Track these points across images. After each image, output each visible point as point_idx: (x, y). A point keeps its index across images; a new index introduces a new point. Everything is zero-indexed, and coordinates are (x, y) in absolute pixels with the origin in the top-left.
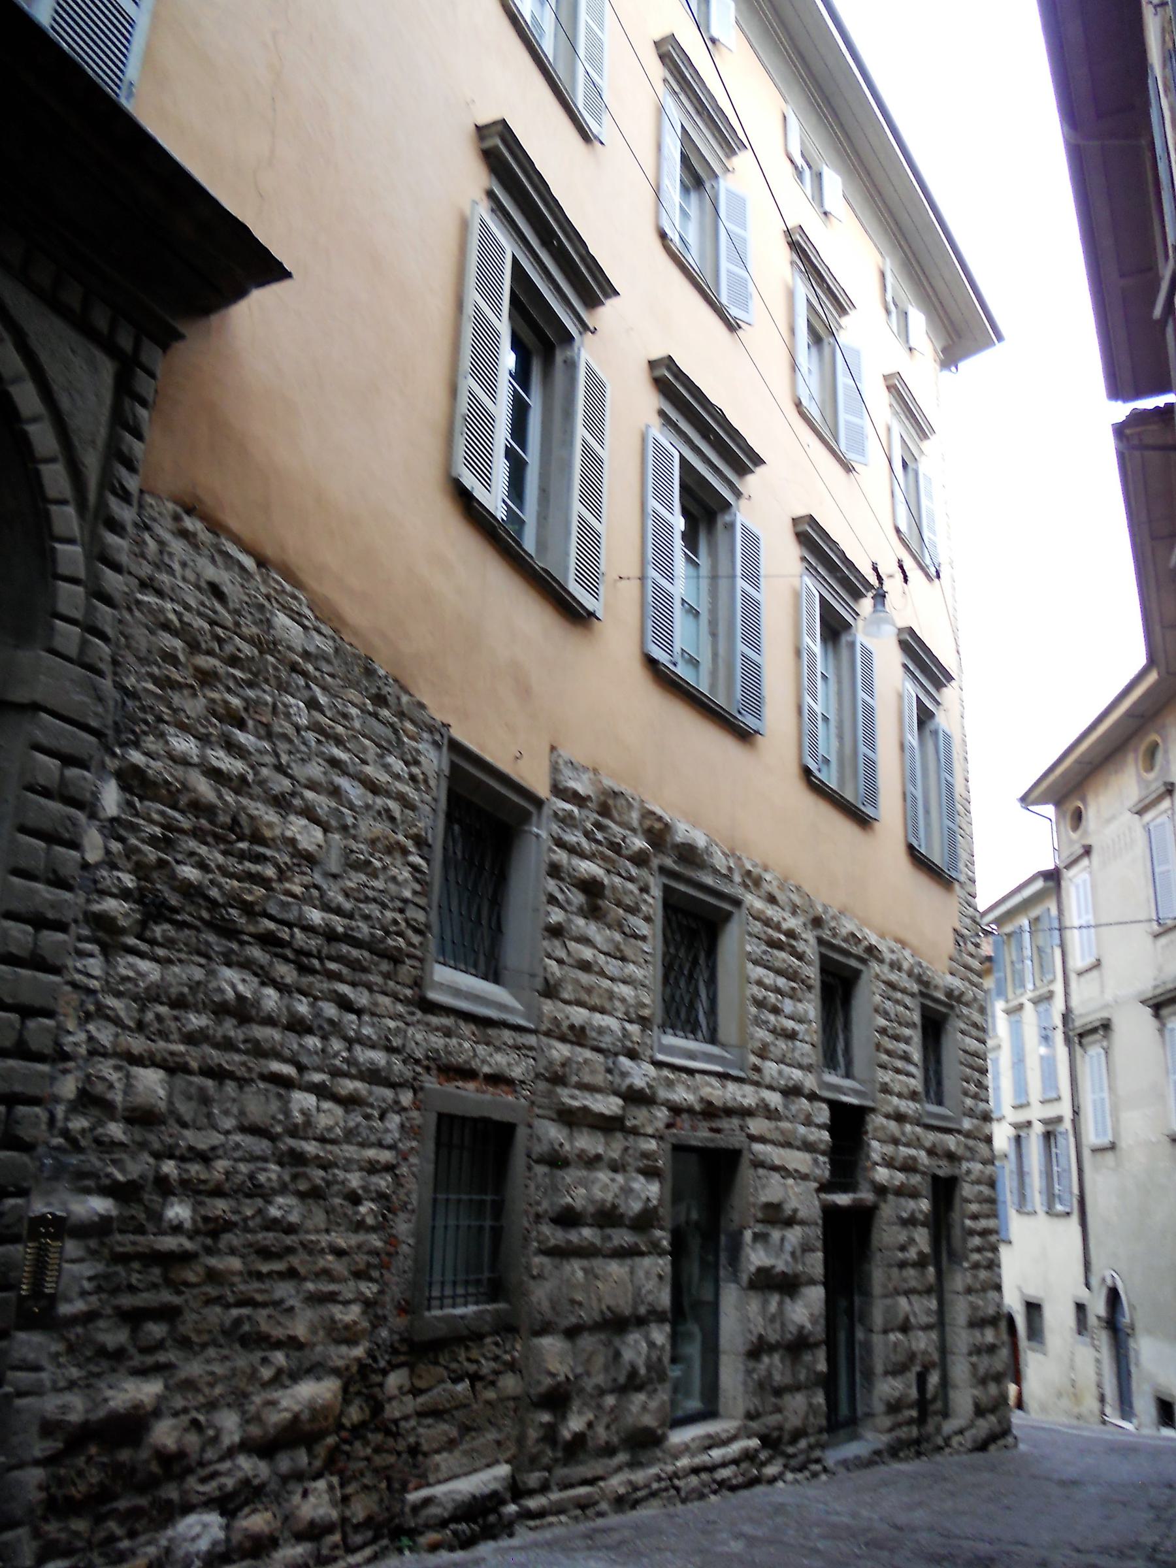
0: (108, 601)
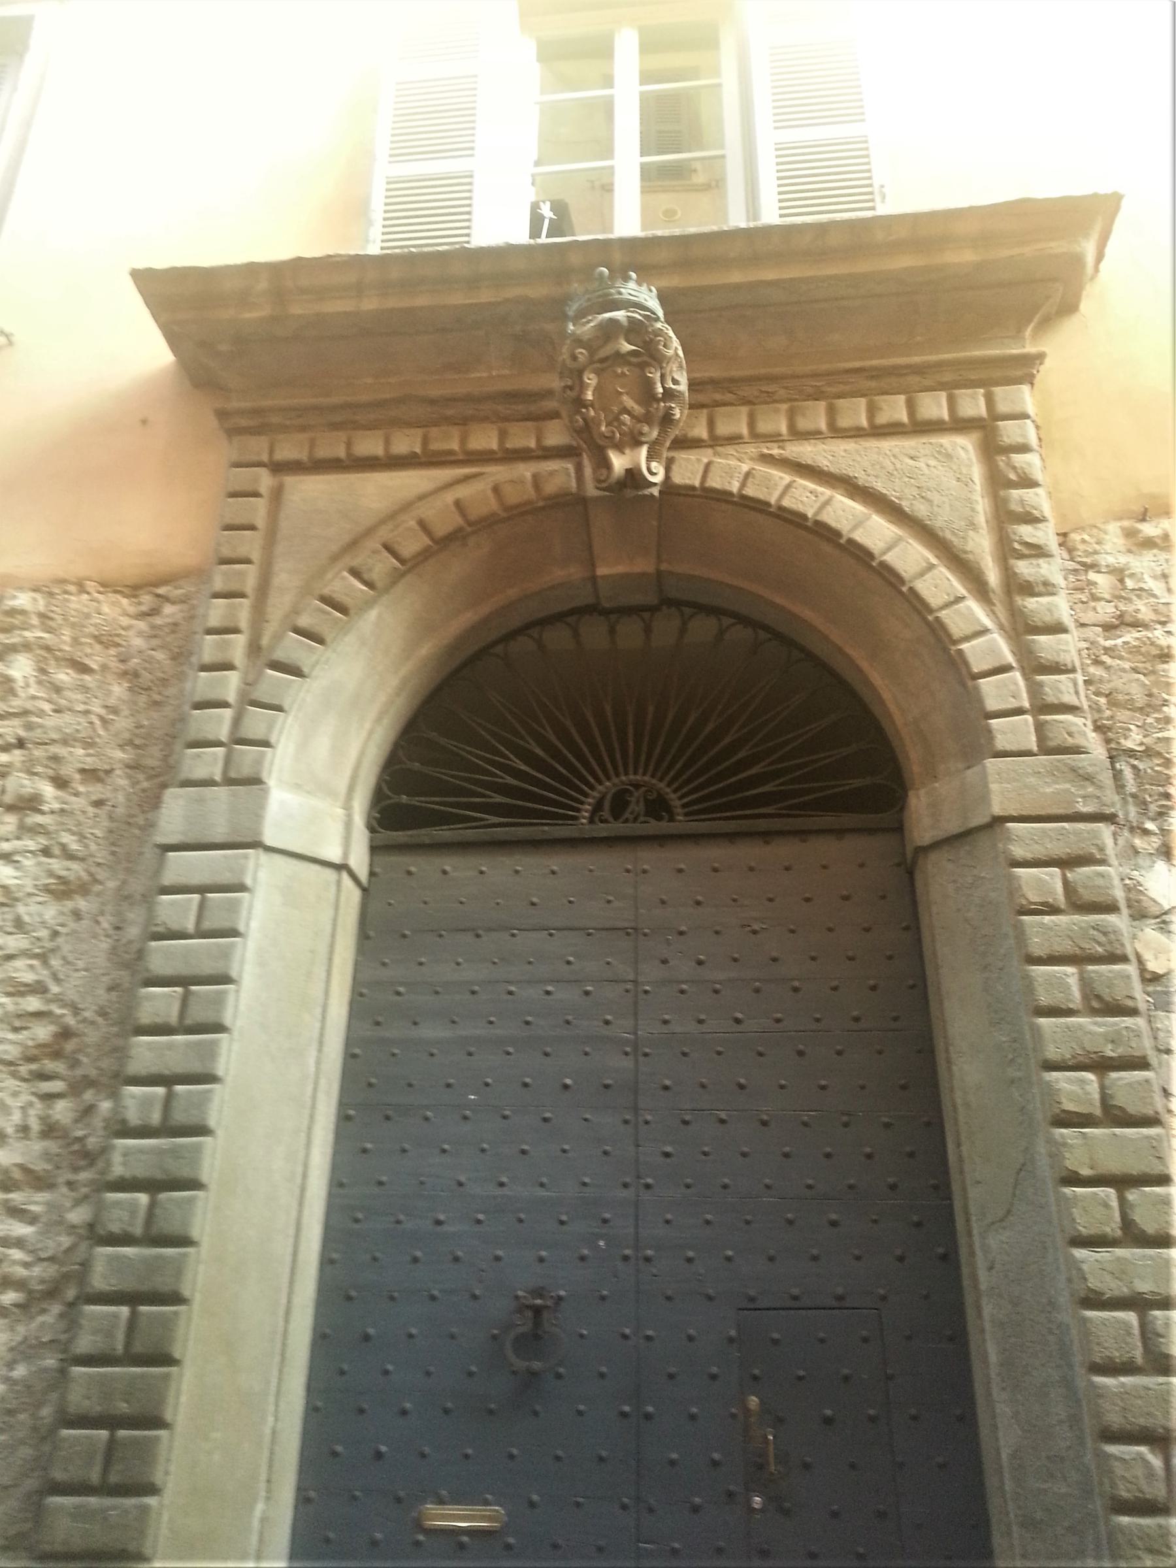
0: (1056, 669)
